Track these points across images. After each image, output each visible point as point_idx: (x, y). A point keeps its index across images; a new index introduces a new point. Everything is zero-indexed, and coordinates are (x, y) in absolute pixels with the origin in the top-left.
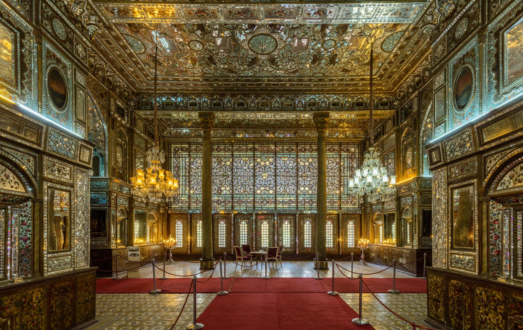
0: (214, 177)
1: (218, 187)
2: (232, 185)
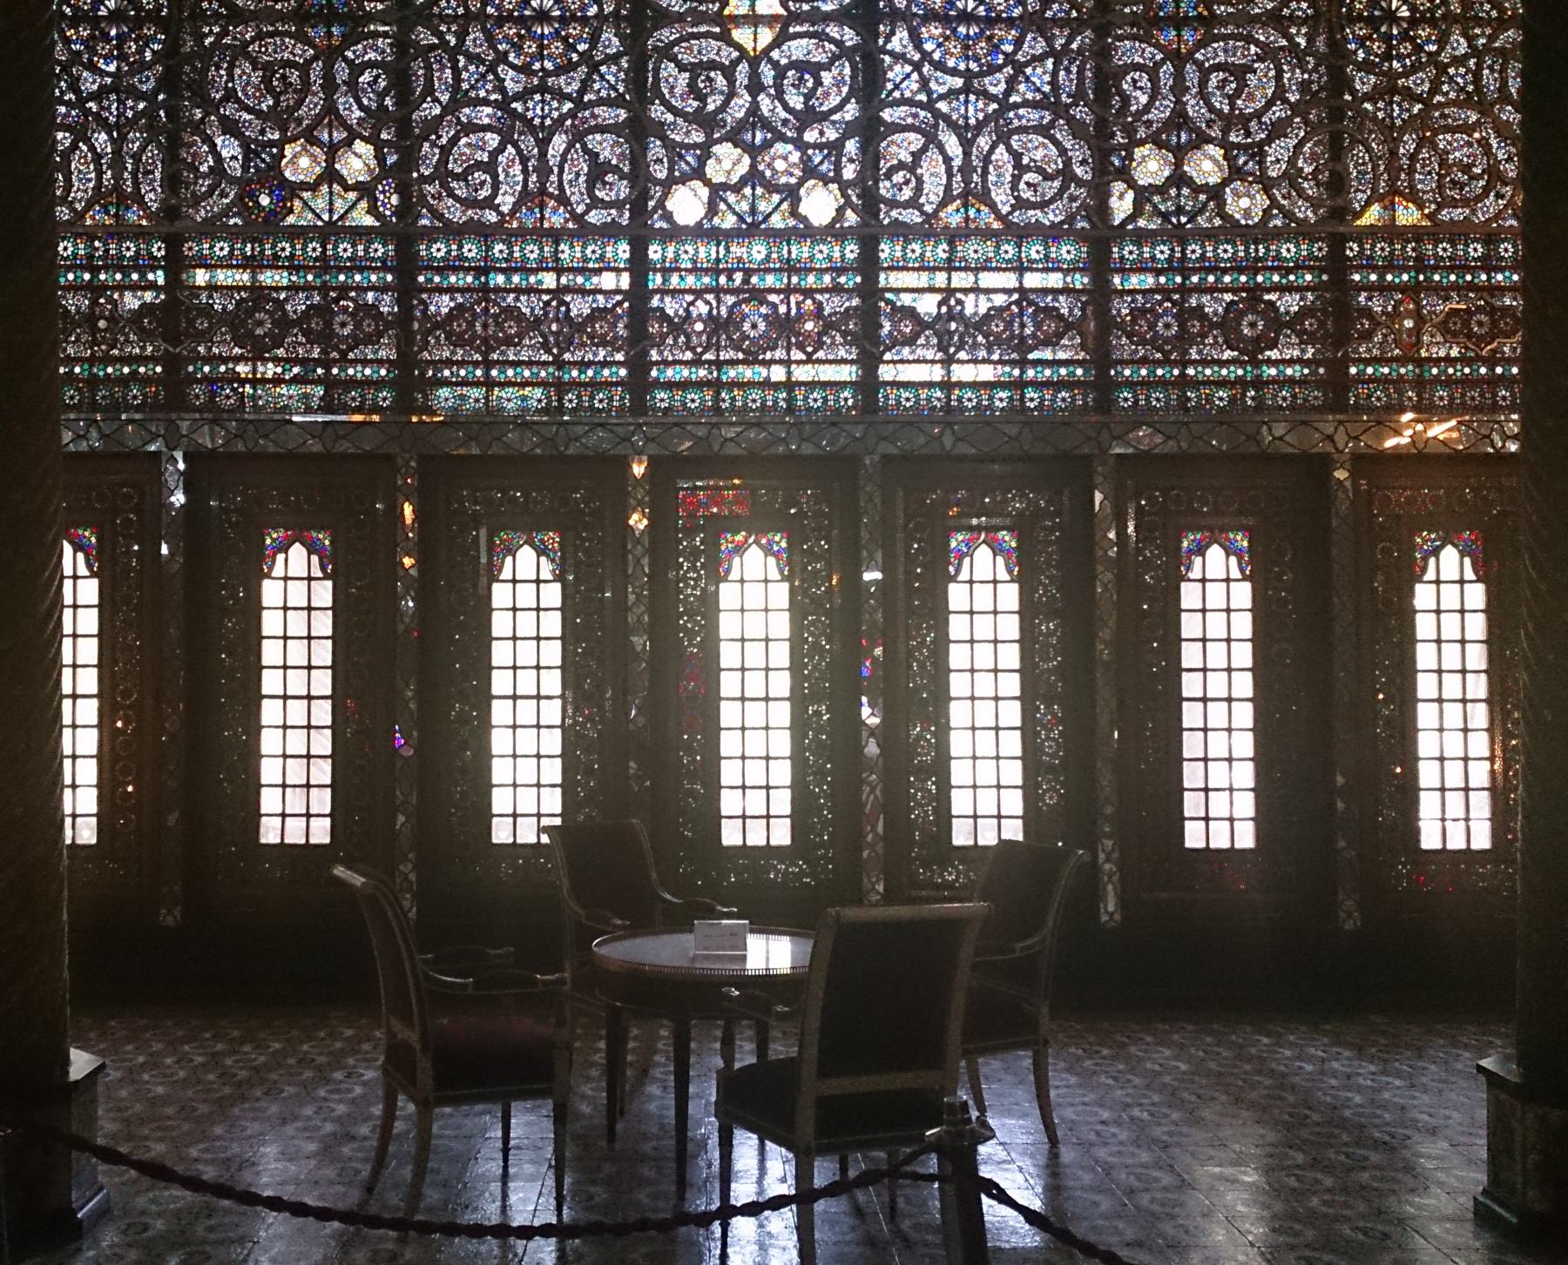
0: (212, 30)
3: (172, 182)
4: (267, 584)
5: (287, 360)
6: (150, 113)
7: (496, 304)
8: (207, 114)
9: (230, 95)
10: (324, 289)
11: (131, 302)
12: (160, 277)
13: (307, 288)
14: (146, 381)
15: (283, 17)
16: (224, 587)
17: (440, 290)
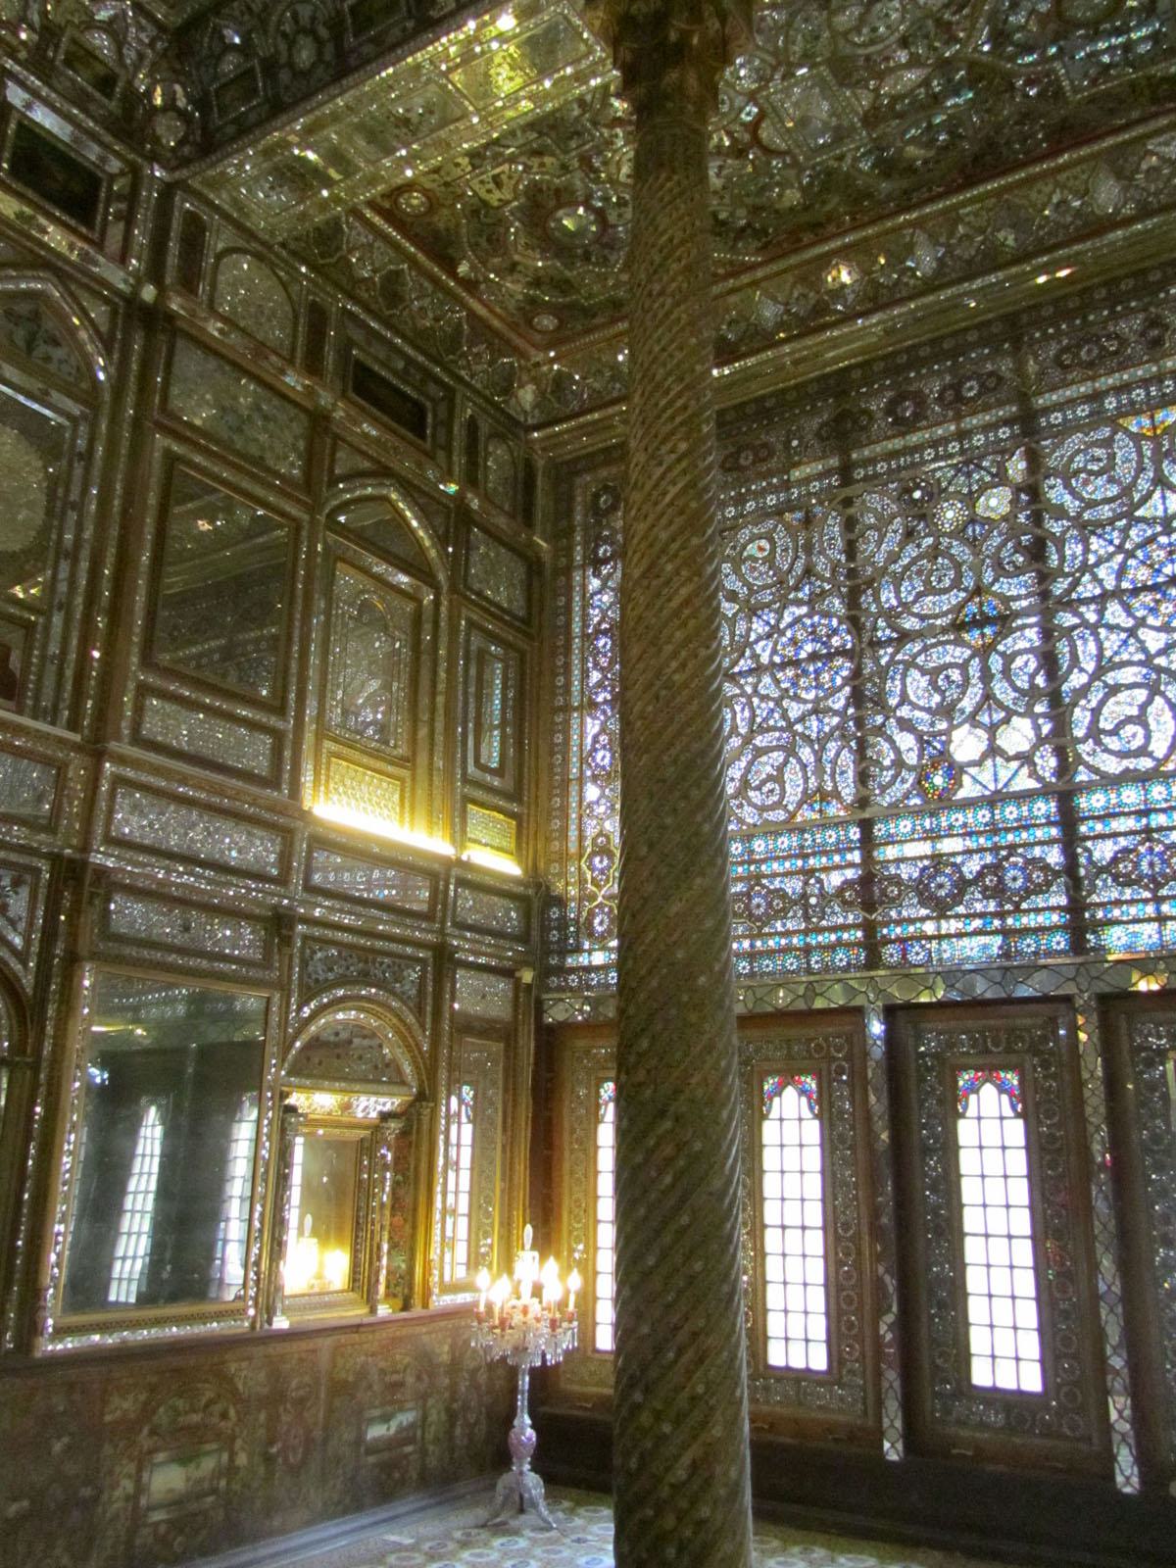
1: (922, 742)
2: (1055, 698)
3: (863, 778)
4: (962, 1124)
5: (967, 916)
6: (841, 727)
7: (1159, 841)
8: (887, 718)
9: (904, 699)
10: (995, 849)
11: (835, 879)
12: (856, 857)
13: (981, 850)
14: (849, 945)
15: (944, 630)
16: (924, 1126)
17: (1102, 837)
